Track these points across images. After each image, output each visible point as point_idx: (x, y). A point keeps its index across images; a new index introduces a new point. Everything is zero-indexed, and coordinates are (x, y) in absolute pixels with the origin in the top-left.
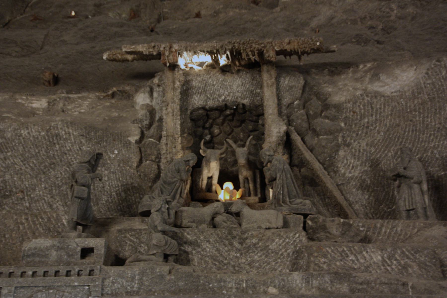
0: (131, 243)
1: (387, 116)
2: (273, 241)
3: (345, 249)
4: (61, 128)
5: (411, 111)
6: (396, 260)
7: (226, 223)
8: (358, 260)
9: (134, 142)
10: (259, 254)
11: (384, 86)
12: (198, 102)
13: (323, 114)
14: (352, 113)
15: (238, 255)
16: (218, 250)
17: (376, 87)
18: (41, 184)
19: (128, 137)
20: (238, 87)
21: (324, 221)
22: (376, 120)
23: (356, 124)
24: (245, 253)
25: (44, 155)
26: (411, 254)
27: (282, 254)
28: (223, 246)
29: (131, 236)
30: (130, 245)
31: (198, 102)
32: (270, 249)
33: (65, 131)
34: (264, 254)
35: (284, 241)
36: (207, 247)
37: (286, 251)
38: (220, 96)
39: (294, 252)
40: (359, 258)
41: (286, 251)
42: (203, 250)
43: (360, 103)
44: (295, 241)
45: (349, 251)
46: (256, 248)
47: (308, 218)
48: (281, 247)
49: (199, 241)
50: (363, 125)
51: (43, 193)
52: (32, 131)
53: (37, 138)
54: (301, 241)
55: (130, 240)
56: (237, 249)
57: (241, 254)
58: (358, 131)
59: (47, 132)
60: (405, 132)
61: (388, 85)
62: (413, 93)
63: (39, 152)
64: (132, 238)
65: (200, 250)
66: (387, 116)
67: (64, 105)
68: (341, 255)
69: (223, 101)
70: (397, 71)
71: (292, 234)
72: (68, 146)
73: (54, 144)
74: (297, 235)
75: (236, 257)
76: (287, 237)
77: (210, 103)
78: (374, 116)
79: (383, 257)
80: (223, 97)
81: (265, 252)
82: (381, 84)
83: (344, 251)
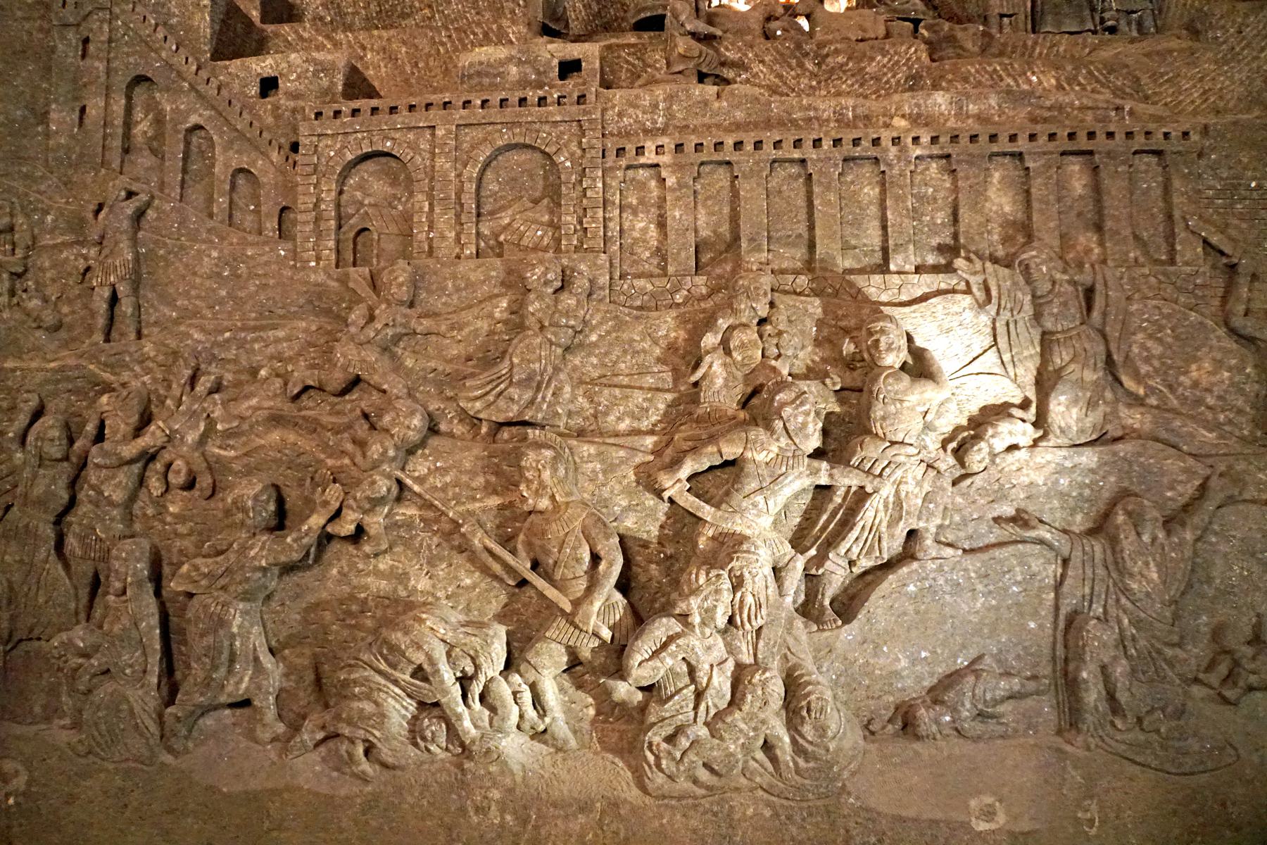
6: (1079, 84)
8: (1018, 85)
10: (849, 82)
15: (814, 83)
16: (780, 76)
27: (887, 82)
37: (894, 76)
41: (894, 76)
42: (753, 77)
57: (819, 83)
75: (811, 87)
79: (1058, 80)
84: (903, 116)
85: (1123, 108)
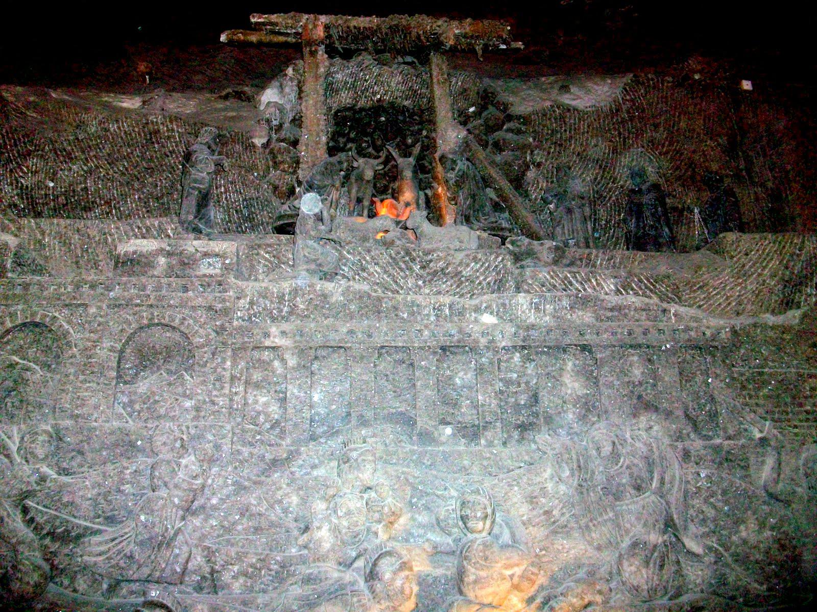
0: (267, 263)
1: (583, 133)
2: (468, 265)
3: (569, 275)
4: (162, 123)
5: (609, 130)
7: (400, 240)
9: (259, 145)
11: (577, 99)
12: (346, 100)
13: (505, 127)
14: (541, 127)
17: (566, 99)
18: (134, 194)
19: (251, 138)
20: (398, 83)
21: (530, 244)
22: (571, 137)
23: (547, 140)
24: (429, 281)
25: (138, 156)
26: (651, 283)
27: (480, 283)
28: (398, 271)
29: (267, 253)
30: (265, 266)
31: (346, 100)
32: (463, 276)
33: (167, 126)
34: (455, 282)
35: (482, 266)
36: (376, 271)
38: (375, 94)
39: (496, 281)
40: (586, 286)
43: (551, 115)
44: (496, 266)
45: (573, 277)
46: (445, 274)
47: (508, 240)
48: (478, 274)
49: (364, 262)
50: (556, 143)
51: (137, 205)
52: (123, 126)
53: (130, 134)
54: (505, 266)
55: (266, 259)
56: (417, 275)
58: (550, 147)
59: (144, 127)
60: (604, 153)
61: (581, 98)
62: (611, 110)
63: (132, 153)
64: (267, 256)
65: (365, 275)
66: (583, 133)
67: (164, 103)
68: (563, 282)
69: (379, 100)
70: (589, 84)
71: (493, 257)
72: (170, 146)
73: (153, 143)
74: (500, 258)
75: (417, 286)
76: (486, 260)
77: (362, 103)
78: (568, 133)
79: (616, 286)
80: (379, 96)
81: (456, 279)
82: (572, 97)
83: (566, 277)
84: (491, 313)
85: (670, 311)
